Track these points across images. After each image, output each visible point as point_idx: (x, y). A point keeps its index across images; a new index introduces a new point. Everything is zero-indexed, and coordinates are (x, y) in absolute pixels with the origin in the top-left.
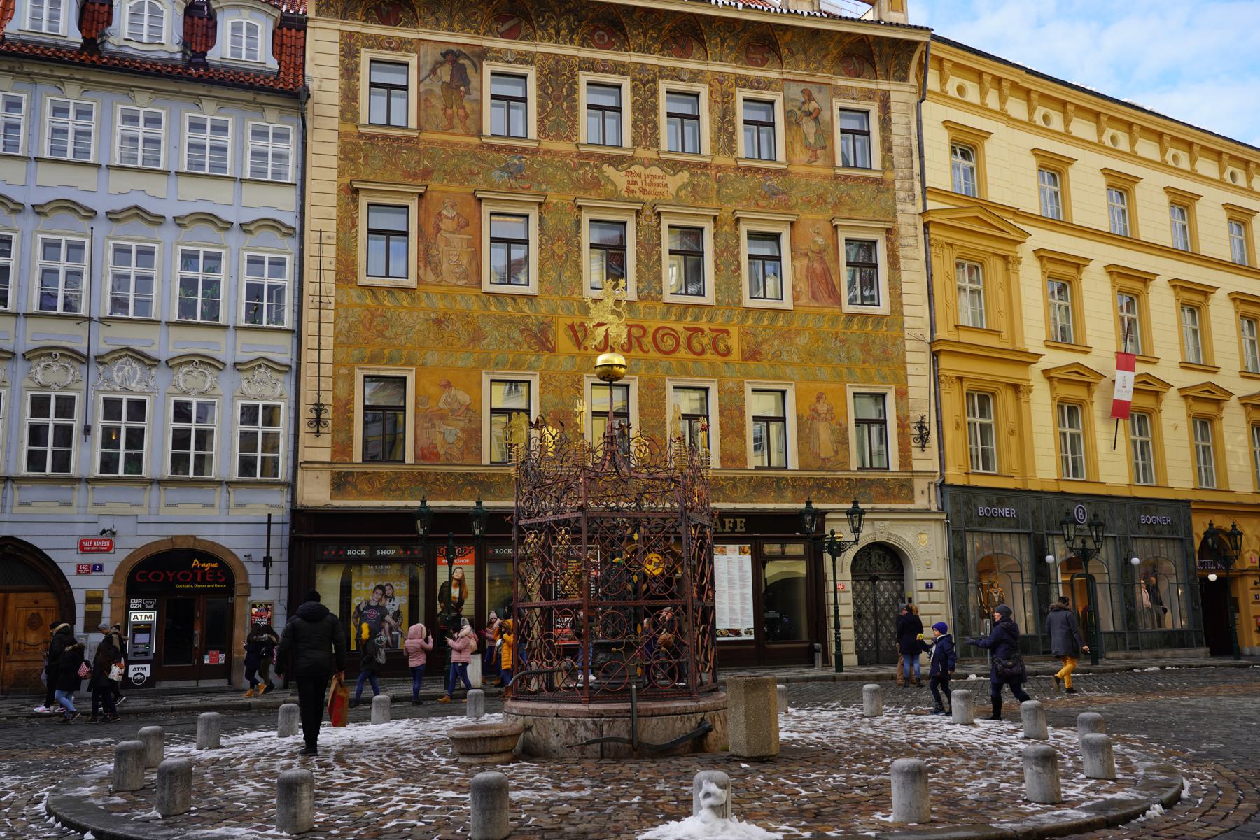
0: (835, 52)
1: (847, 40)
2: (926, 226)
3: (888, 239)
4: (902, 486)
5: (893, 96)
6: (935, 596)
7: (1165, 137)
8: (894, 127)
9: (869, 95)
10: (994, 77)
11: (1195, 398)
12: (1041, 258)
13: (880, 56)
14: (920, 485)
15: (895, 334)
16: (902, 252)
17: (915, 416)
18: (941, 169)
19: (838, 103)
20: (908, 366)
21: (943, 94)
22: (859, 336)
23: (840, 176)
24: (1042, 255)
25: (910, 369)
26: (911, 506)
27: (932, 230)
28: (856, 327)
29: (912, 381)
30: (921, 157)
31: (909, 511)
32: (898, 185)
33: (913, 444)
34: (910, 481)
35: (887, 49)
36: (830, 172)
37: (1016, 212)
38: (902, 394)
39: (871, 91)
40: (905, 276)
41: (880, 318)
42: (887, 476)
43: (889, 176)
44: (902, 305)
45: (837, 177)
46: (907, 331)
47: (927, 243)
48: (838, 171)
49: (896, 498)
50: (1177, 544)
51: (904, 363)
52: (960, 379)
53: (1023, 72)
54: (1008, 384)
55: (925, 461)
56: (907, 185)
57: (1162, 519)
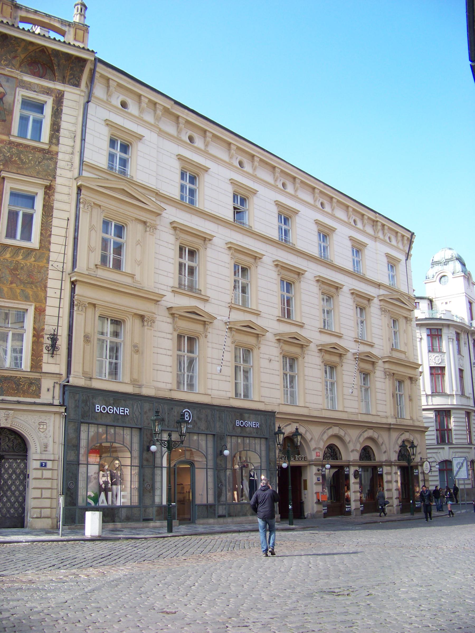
0: (23, 56)
1: (31, 48)
2: (79, 189)
3: (46, 193)
4: (31, 383)
5: (66, 95)
6: (47, 474)
7: (277, 169)
8: (64, 117)
9: (48, 92)
10: (150, 101)
11: (286, 342)
12: (175, 228)
13: (59, 65)
14: (46, 383)
15: (41, 264)
16: (56, 205)
17: (49, 329)
18: (98, 152)
19: (21, 93)
20: (48, 290)
21: (108, 102)
22: (11, 262)
23: (13, 142)
24: (176, 227)
25: (50, 292)
26: (37, 400)
27: (83, 192)
28: (8, 256)
29: (50, 302)
30: (83, 140)
31: (35, 404)
32: (60, 156)
33: (45, 351)
34: (39, 380)
35: (63, 61)
36: (5, 138)
37: (157, 194)
38: (40, 312)
39: (49, 89)
40: (55, 222)
41: (30, 251)
42: (19, 374)
43: (54, 148)
44: (50, 243)
45: (11, 143)
46: (51, 263)
47: (78, 202)
48: (12, 139)
49: (25, 393)
50: (263, 441)
51: (46, 287)
52: (94, 305)
53: (173, 103)
54: (136, 314)
55: (53, 365)
56: (67, 157)
57: (252, 424)
